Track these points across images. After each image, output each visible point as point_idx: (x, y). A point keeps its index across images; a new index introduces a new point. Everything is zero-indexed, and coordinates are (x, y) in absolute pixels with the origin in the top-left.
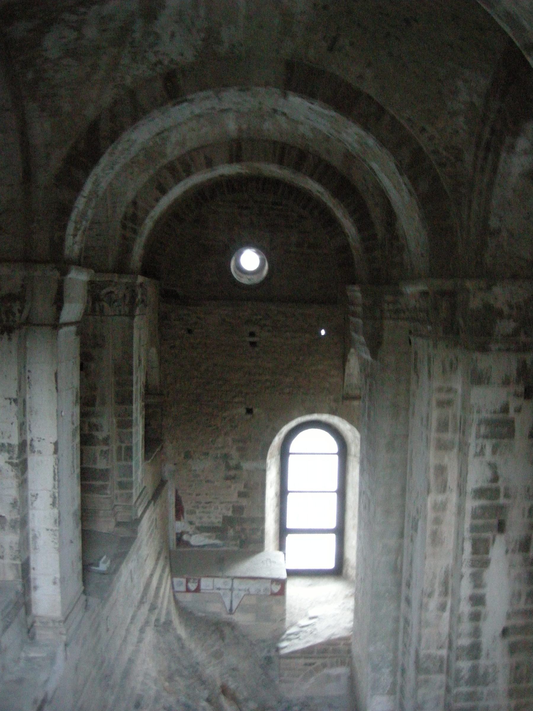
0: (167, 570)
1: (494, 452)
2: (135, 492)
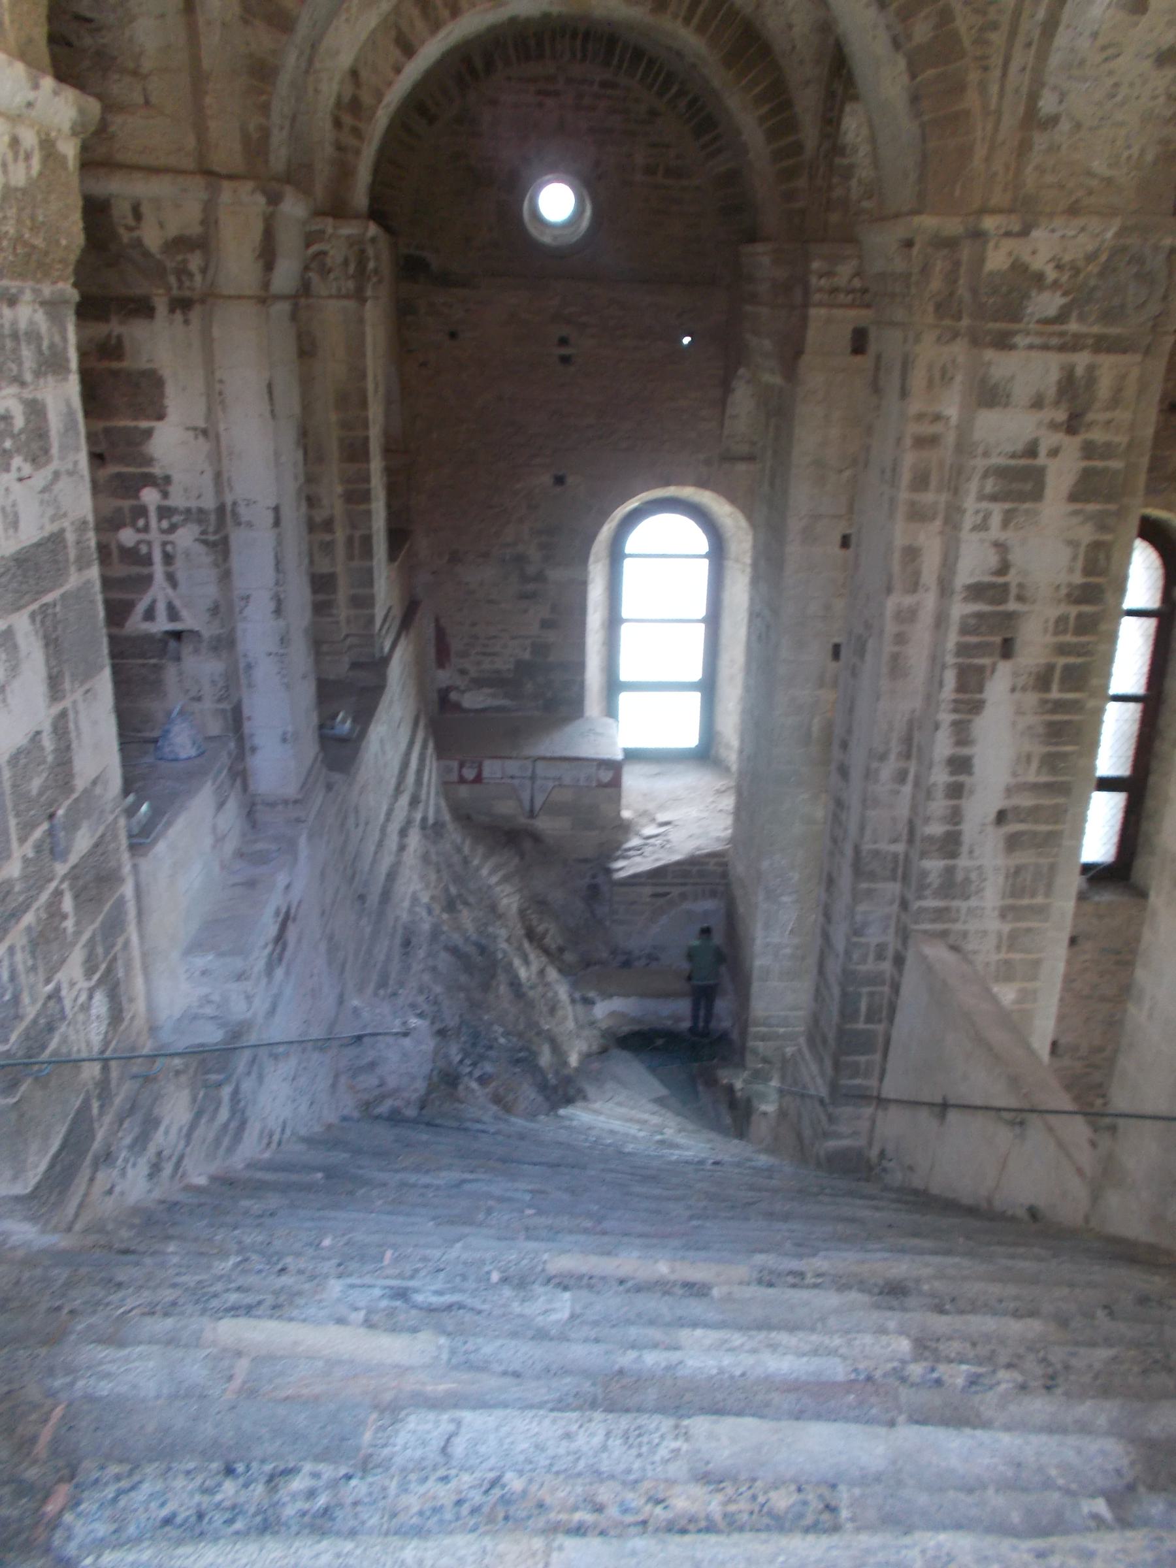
0: (431, 745)
1: (1005, 524)
2: (379, 612)
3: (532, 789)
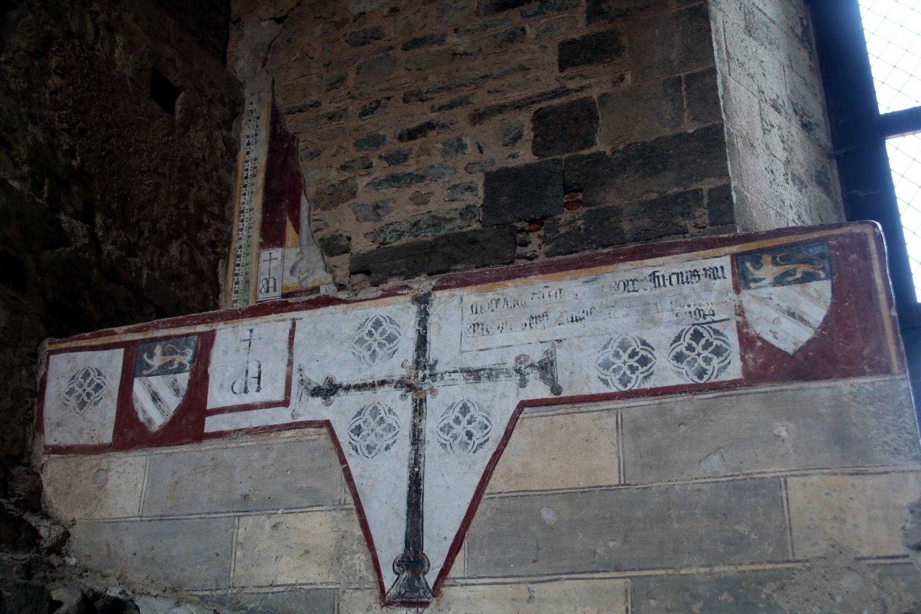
3: (417, 439)
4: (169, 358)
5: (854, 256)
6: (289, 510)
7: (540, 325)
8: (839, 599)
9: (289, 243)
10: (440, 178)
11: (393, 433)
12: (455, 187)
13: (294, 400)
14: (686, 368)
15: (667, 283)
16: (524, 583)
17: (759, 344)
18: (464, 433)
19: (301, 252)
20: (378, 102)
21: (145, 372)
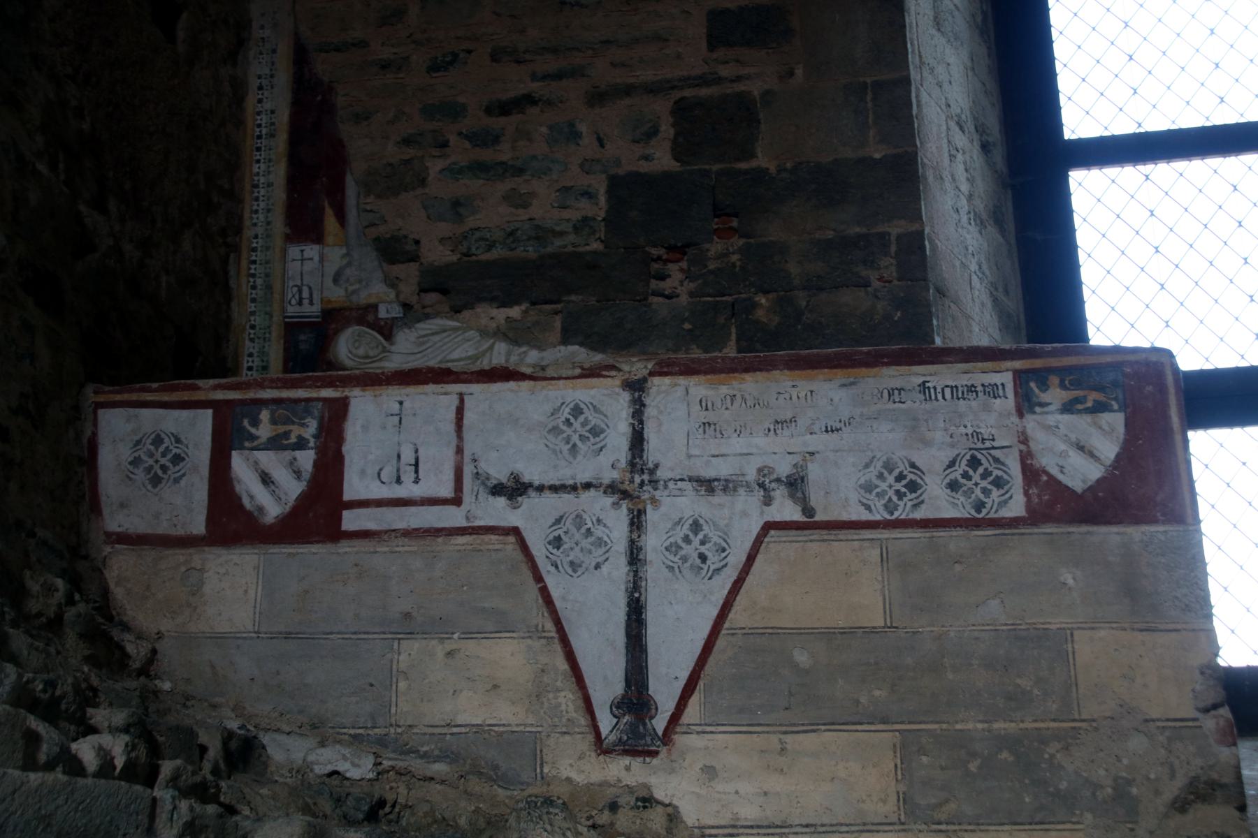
3: (635, 557)
4: (282, 429)
5: (1150, 388)
6: (468, 635)
7: (787, 432)
8: (1125, 761)
9: (330, 239)
10: (545, 174)
11: (604, 549)
12: (566, 189)
13: (467, 497)
14: (962, 499)
15: (940, 396)
16: (774, 733)
17: (1045, 478)
18: (695, 555)
19: (347, 254)
20: (455, 56)
21: (247, 444)
